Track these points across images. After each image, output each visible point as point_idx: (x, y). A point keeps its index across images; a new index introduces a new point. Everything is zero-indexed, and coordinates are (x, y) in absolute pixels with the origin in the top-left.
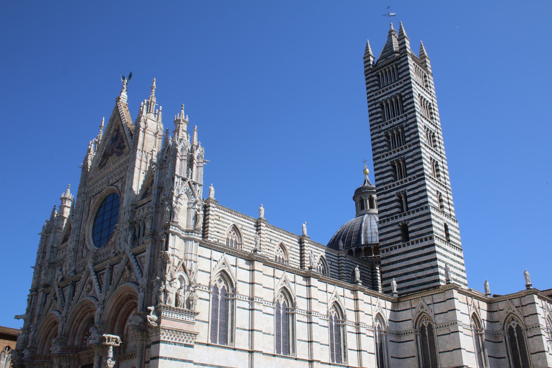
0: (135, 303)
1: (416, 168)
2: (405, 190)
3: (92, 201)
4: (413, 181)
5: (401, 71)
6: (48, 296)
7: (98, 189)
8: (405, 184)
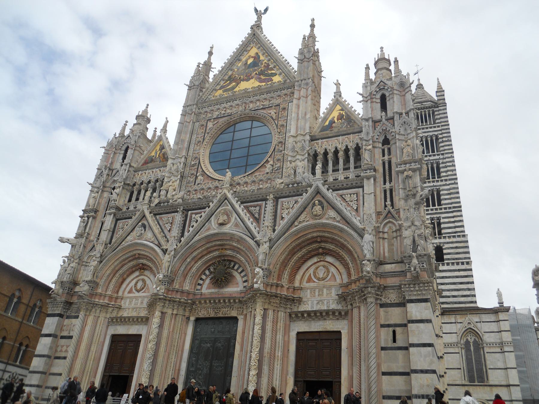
0: (323, 248)
1: (453, 201)
2: (440, 217)
3: (210, 125)
4: (448, 210)
5: (438, 117)
6: (118, 222)
7: (223, 112)
8: (439, 211)
